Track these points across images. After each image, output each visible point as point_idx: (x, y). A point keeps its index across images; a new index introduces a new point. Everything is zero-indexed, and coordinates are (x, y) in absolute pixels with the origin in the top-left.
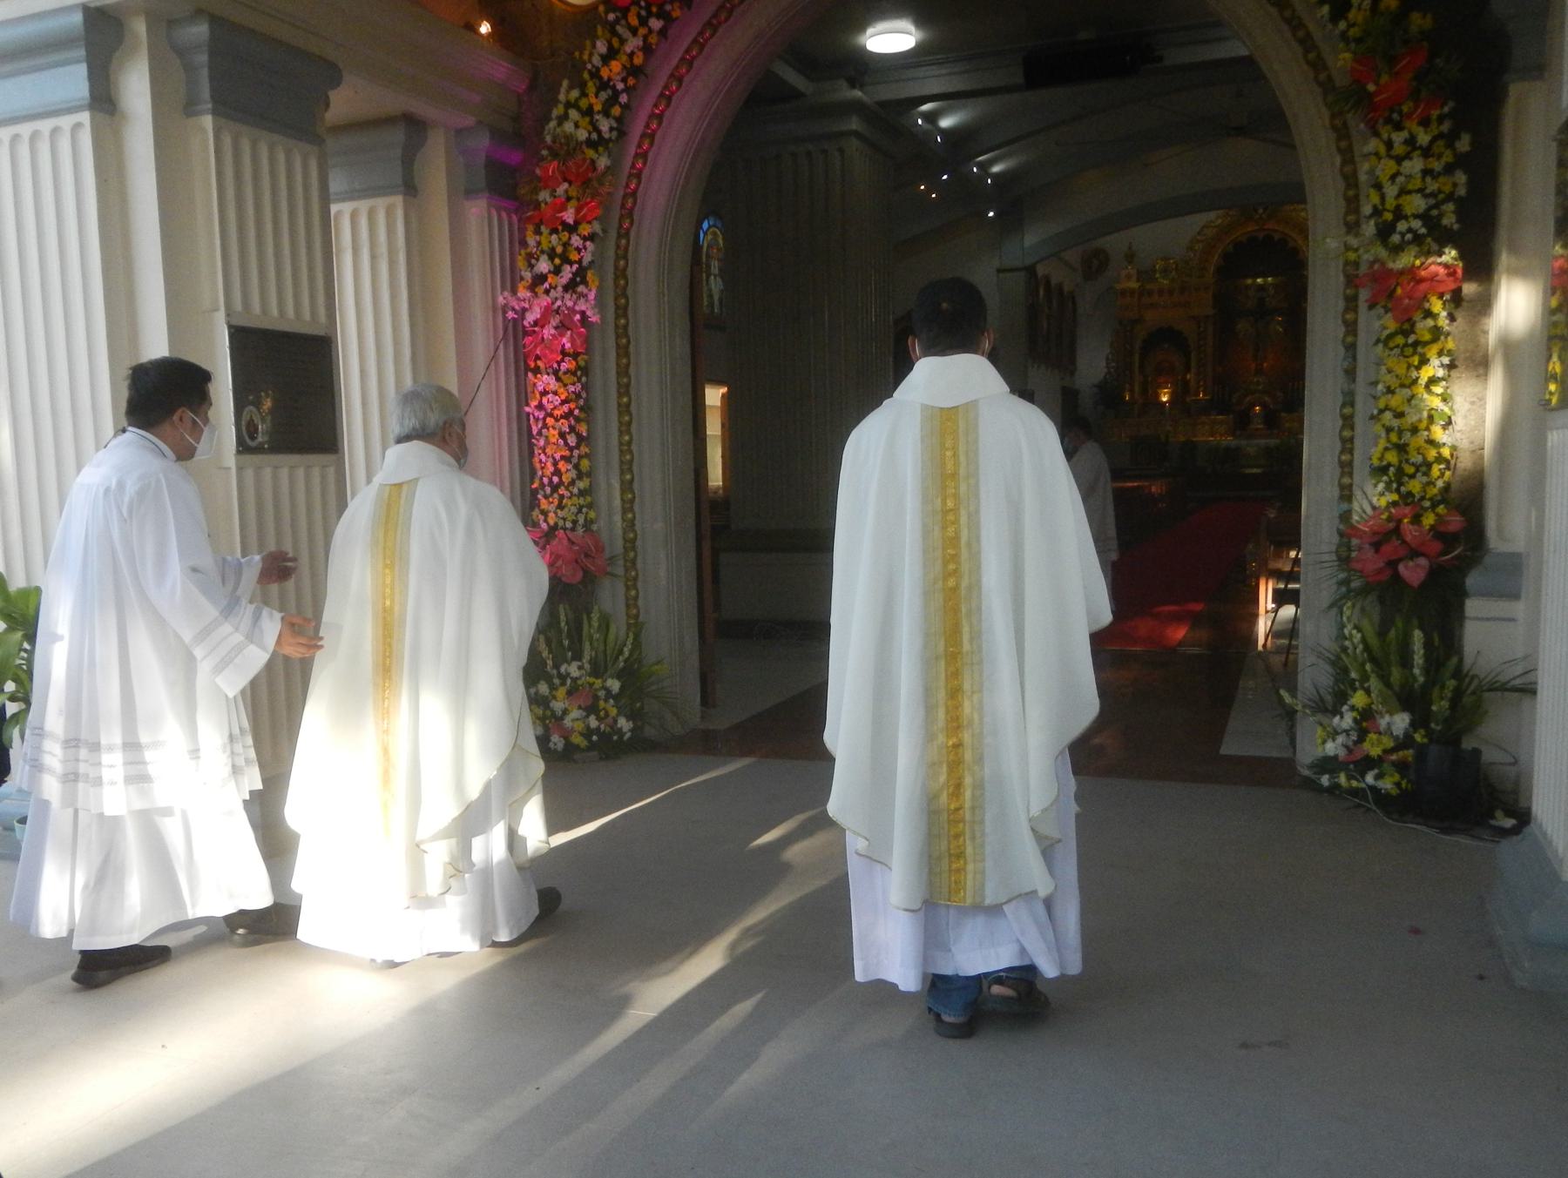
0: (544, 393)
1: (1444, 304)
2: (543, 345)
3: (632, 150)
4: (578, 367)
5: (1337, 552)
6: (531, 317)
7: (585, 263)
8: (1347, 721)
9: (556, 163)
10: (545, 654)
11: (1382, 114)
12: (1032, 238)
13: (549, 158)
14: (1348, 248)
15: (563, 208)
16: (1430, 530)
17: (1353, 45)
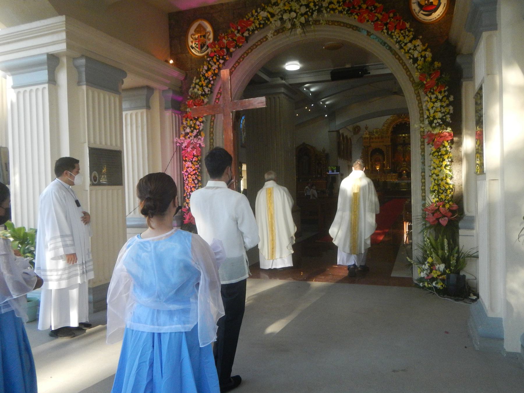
0: (188, 167)
1: (449, 143)
2: (187, 154)
3: (215, 97)
4: (198, 160)
5: (422, 216)
6: (184, 145)
7: (201, 129)
8: (427, 266)
9: (192, 100)
11: (428, 90)
12: (338, 122)
13: (190, 99)
14: (421, 127)
16: (448, 209)
17: (419, 71)
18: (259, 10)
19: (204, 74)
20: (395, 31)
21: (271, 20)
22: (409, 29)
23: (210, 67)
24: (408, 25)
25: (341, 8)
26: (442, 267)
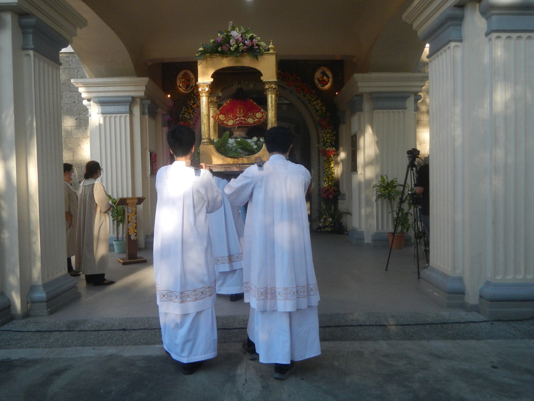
3: (194, 120)
8: (322, 220)
9: (183, 122)
19: (191, 106)
23: (195, 101)
24: (314, 92)
26: (331, 219)
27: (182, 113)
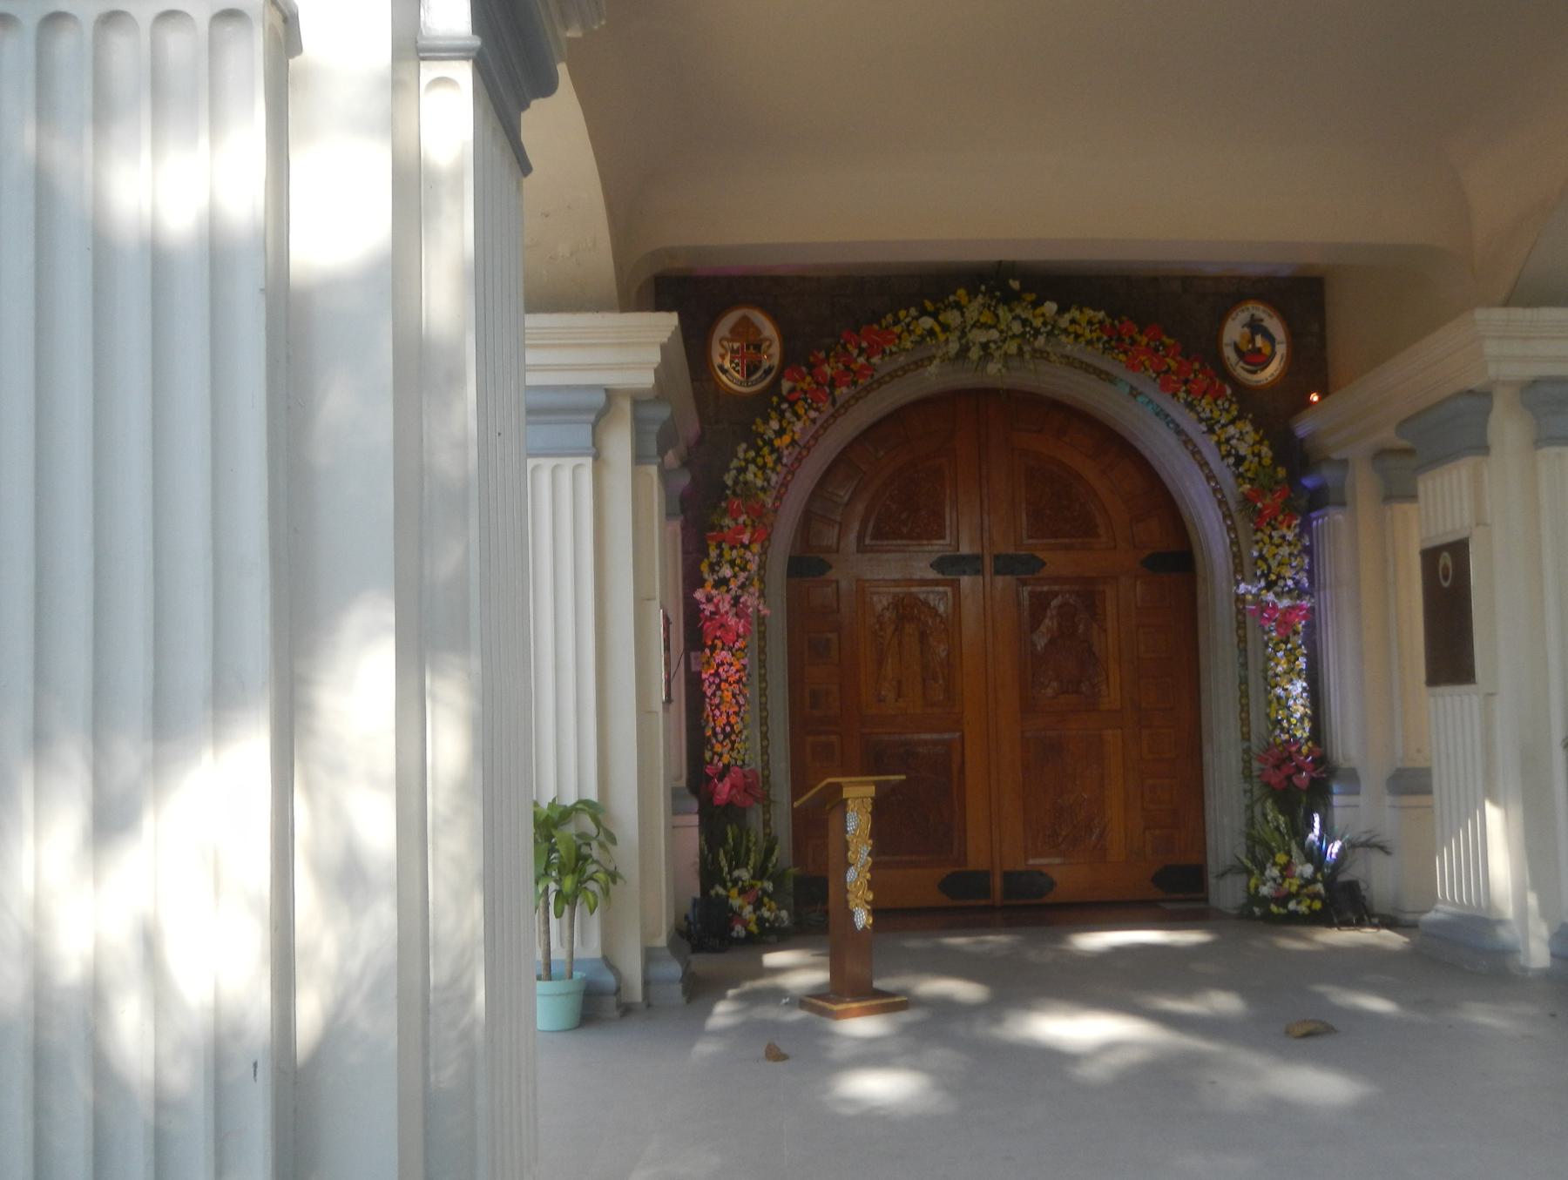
7: (752, 572)
8: (1274, 872)
10: (724, 863)
15: (743, 533)
17: (1247, 481)
18: (913, 311)
20: (1203, 398)
21: (942, 337)
22: (1229, 397)
23: (785, 424)
24: (1229, 391)
25: (1094, 335)
27: (735, 468)
